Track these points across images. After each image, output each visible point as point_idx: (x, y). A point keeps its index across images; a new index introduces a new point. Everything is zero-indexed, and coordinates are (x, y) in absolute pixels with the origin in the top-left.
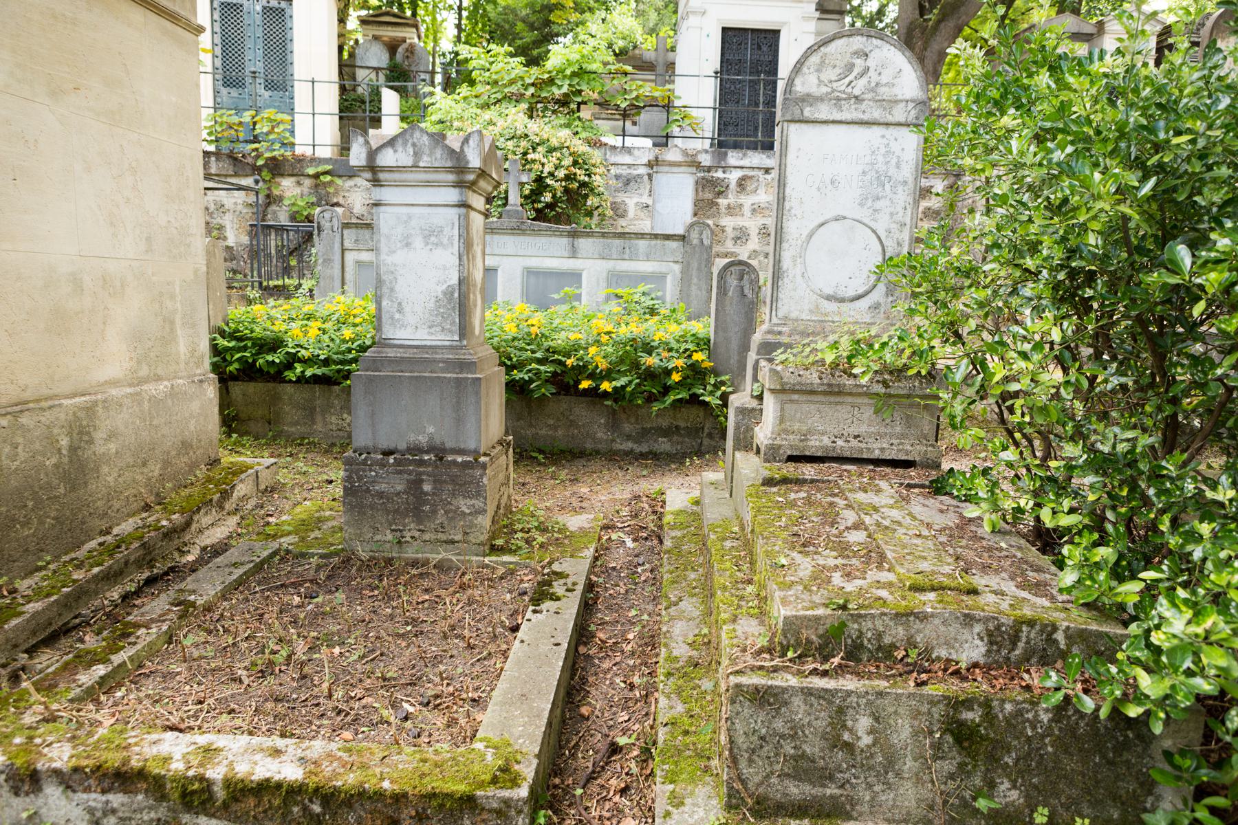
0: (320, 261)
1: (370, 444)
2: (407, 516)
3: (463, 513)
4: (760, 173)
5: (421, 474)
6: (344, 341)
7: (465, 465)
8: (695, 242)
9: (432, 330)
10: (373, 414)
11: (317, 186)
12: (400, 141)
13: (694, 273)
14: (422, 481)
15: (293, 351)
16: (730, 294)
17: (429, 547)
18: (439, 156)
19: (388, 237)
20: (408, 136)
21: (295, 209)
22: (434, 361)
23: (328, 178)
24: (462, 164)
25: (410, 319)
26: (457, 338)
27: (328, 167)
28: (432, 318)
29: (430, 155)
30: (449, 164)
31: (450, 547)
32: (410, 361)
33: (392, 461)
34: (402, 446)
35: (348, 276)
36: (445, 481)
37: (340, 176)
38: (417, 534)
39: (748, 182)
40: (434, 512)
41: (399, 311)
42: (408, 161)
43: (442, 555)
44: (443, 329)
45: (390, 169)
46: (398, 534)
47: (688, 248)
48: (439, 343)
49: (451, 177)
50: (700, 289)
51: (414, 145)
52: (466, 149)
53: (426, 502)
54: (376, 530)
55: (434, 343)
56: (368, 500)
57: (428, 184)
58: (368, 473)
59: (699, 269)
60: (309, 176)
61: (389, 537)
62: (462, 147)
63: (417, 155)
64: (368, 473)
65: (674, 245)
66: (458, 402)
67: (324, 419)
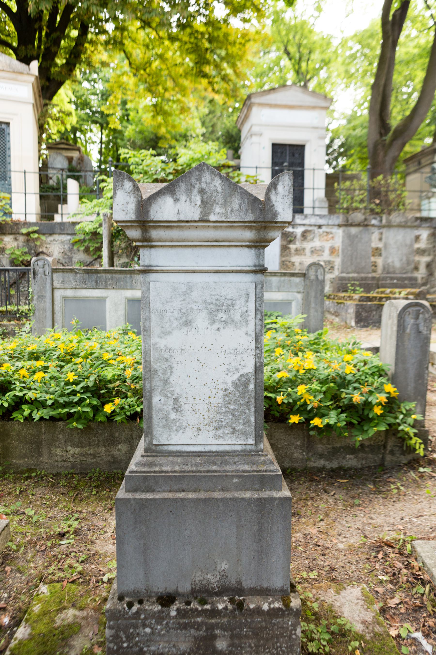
0: (35, 297)
1: (141, 587)
4: (315, 229)
5: (212, 627)
6: (67, 383)
7: (273, 613)
8: (313, 277)
9: (220, 432)
11: (28, 241)
13: (312, 300)
14: (215, 637)
15: (21, 394)
16: (408, 330)
19: (160, 314)
20: (193, 180)
21: (13, 256)
23: (36, 236)
24: (269, 217)
26: (251, 441)
27: (36, 228)
28: (218, 417)
29: (225, 205)
30: (250, 217)
33: (173, 613)
35: (57, 308)
36: (247, 637)
37: (44, 234)
39: (308, 234)
41: (176, 409)
44: (234, 431)
47: (308, 282)
48: (228, 448)
49: (249, 235)
50: (316, 311)
51: (202, 192)
52: (273, 197)
55: (221, 448)
59: (316, 297)
60: (22, 234)
65: (297, 280)
66: (260, 530)
67: (50, 451)
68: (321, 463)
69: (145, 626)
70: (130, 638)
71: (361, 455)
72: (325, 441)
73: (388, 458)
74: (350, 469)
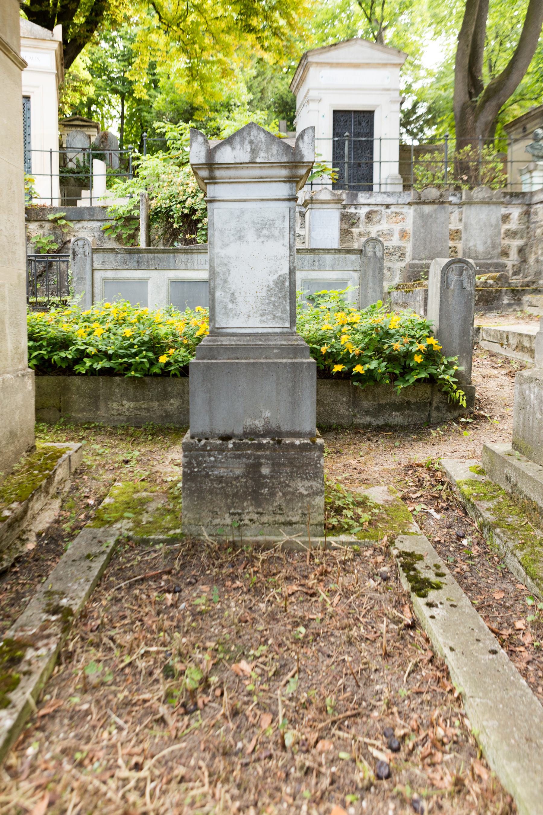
0: (75, 280)
1: (207, 429)
2: (246, 499)
3: (301, 495)
6: (125, 338)
7: (303, 447)
8: (370, 254)
9: (264, 318)
10: (210, 401)
11: (54, 228)
12: (238, 139)
13: (370, 279)
14: (260, 464)
15: (83, 348)
17: (267, 529)
18: (275, 151)
19: (222, 232)
21: (39, 245)
22: (269, 347)
23: (64, 222)
24: (298, 159)
25: (243, 307)
26: (287, 325)
27: (63, 214)
28: (263, 307)
29: (267, 151)
30: (285, 159)
31: (288, 528)
32: (245, 348)
33: (231, 446)
34: (239, 431)
35: (97, 291)
36: (284, 464)
37: (71, 221)
38: (255, 517)
39: (374, 215)
40: (273, 494)
41: (232, 301)
42: (246, 158)
43: (286, 538)
44: (275, 317)
45: (228, 166)
46: (237, 517)
47: (365, 260)
48: (270, 330)
49: (284, 172)
50: (375, 291)
51: (251, 142)
52: (301, 144)
53: (264, 485)
54: (215, 514)
55: (265, 331)
56: (207, 485)
57: (261, 180)
58: (207, 459)
59: (374, 276)
60: (49, 221)
61: (228, 521)
62: (297, 143)
63: (254, 151)
64: (207, 459)
65: (353, 257)
66: (293, 386)
67: (107, 405)
68: (368, 419)
69: (210, 456)
70: (199, 464)
71: (406, 412)
72: (370, 398)
73: (434, 414)
74: (396, 425)
